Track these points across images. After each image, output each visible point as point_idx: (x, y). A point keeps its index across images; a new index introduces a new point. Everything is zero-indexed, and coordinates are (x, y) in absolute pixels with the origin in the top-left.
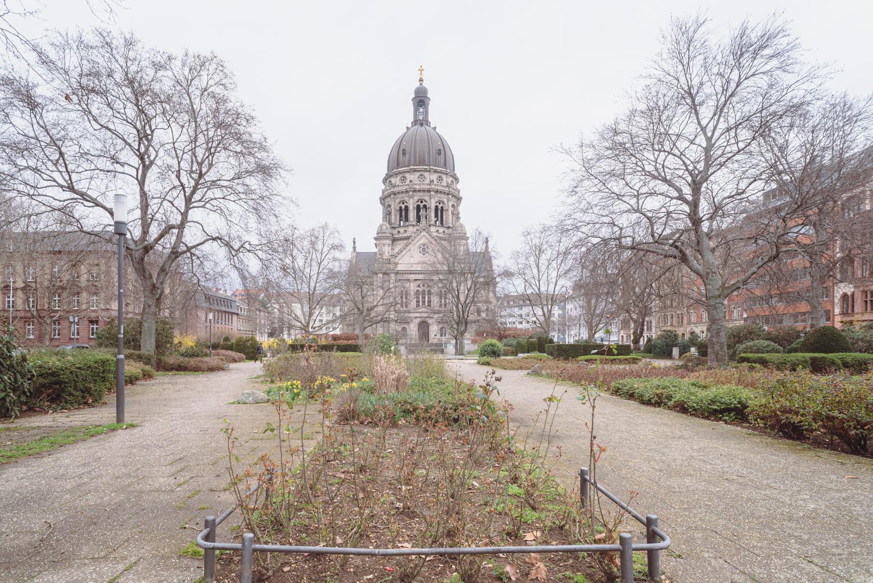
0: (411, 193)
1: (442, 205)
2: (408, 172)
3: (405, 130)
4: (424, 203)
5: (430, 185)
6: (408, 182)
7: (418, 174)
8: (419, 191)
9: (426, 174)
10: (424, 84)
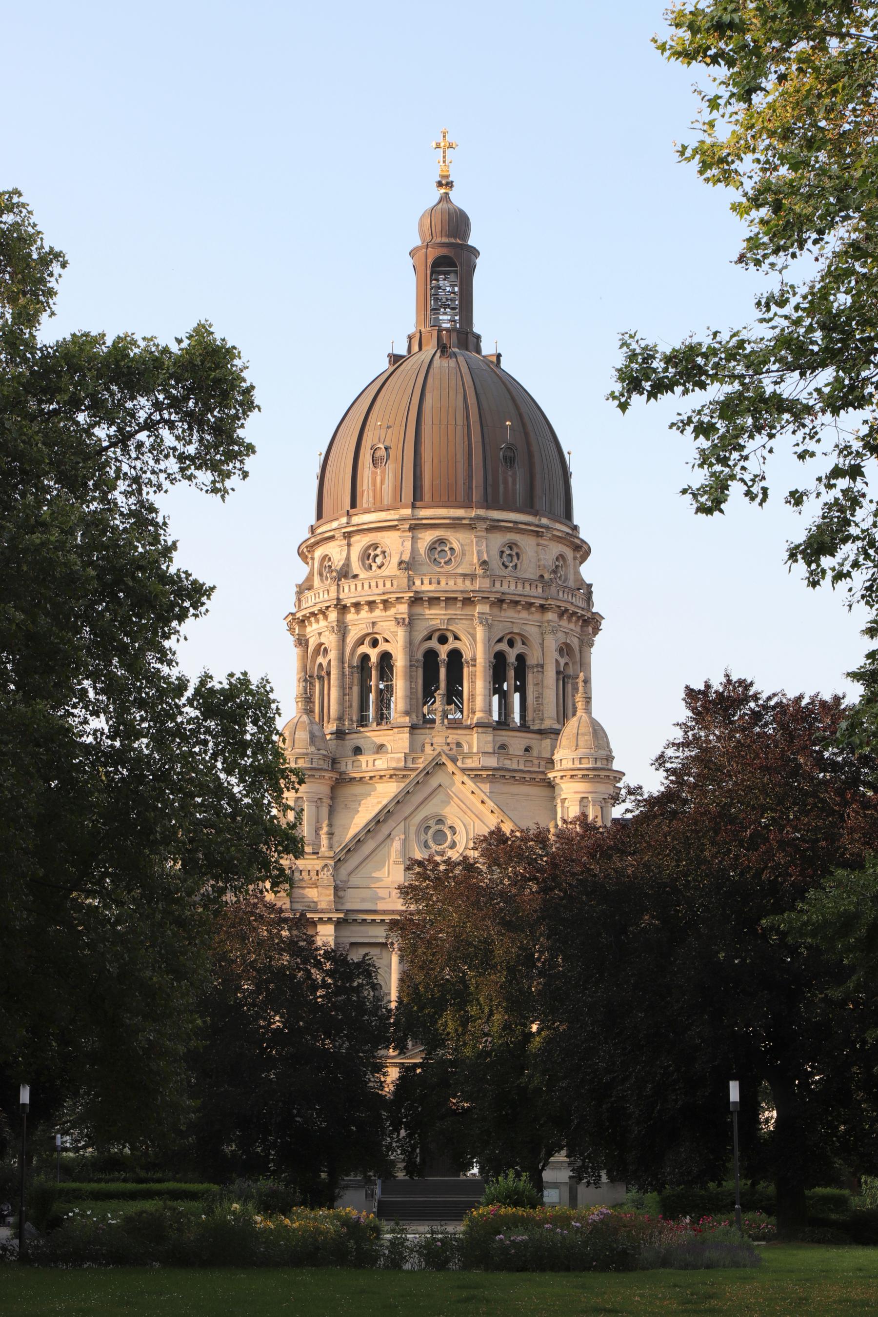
1: (519, 648)
3: (384, 365)
4: (452, 644)
7: (427, 537)
8: (434, 601)
10: (459, 199)
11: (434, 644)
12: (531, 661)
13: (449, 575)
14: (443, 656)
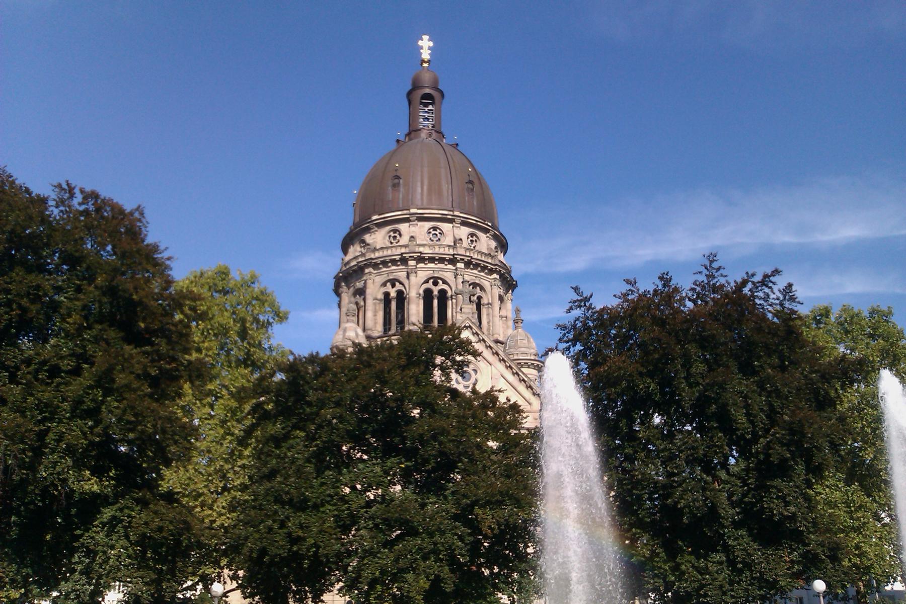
0: (412, 263)
2: (407, 220)
4: (441, 286)
5: (454, 247)
6: (404, 240)
8: (432, 260)
9: (445, 227)
11: (430, 285)
12: (484, 301)
13: (440, 246)
14: (436, 293)
